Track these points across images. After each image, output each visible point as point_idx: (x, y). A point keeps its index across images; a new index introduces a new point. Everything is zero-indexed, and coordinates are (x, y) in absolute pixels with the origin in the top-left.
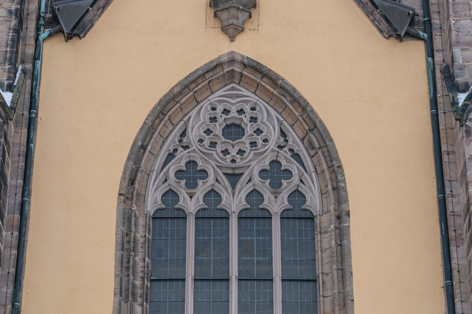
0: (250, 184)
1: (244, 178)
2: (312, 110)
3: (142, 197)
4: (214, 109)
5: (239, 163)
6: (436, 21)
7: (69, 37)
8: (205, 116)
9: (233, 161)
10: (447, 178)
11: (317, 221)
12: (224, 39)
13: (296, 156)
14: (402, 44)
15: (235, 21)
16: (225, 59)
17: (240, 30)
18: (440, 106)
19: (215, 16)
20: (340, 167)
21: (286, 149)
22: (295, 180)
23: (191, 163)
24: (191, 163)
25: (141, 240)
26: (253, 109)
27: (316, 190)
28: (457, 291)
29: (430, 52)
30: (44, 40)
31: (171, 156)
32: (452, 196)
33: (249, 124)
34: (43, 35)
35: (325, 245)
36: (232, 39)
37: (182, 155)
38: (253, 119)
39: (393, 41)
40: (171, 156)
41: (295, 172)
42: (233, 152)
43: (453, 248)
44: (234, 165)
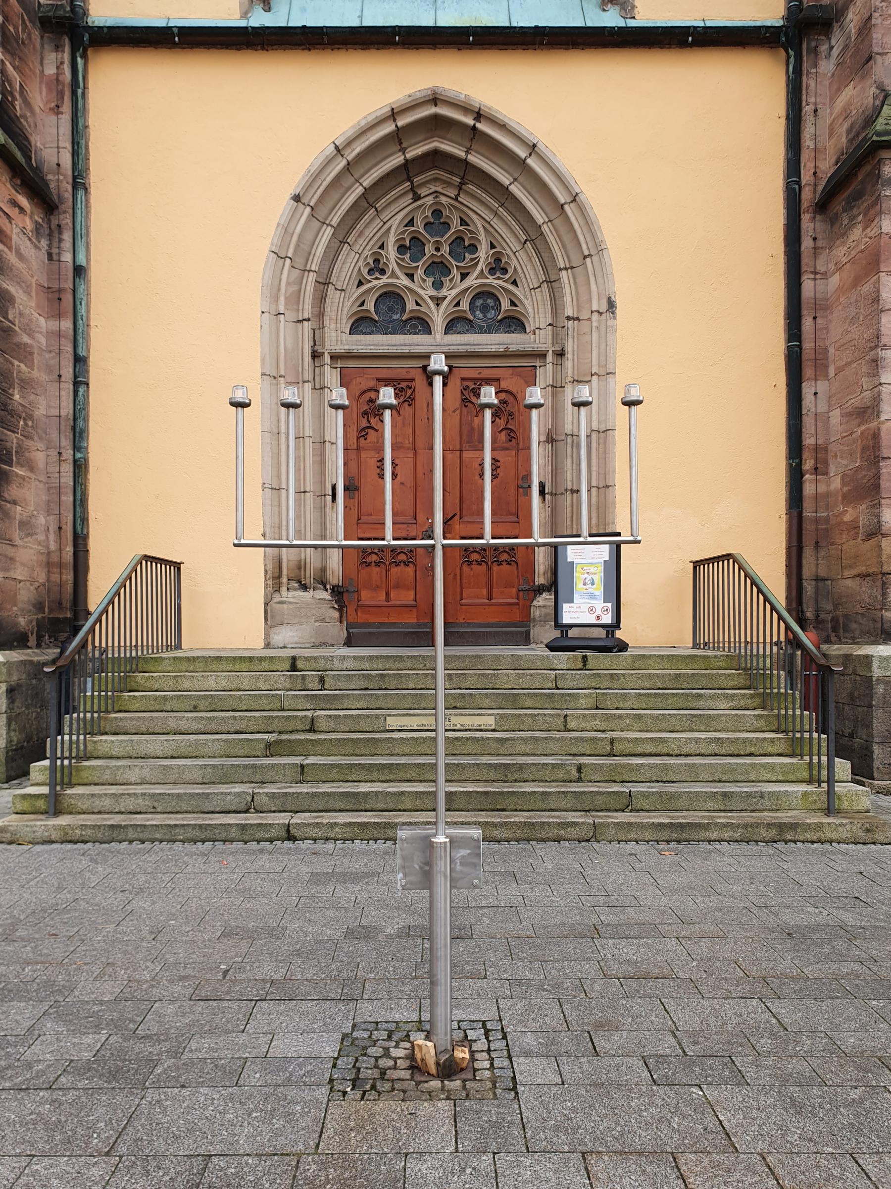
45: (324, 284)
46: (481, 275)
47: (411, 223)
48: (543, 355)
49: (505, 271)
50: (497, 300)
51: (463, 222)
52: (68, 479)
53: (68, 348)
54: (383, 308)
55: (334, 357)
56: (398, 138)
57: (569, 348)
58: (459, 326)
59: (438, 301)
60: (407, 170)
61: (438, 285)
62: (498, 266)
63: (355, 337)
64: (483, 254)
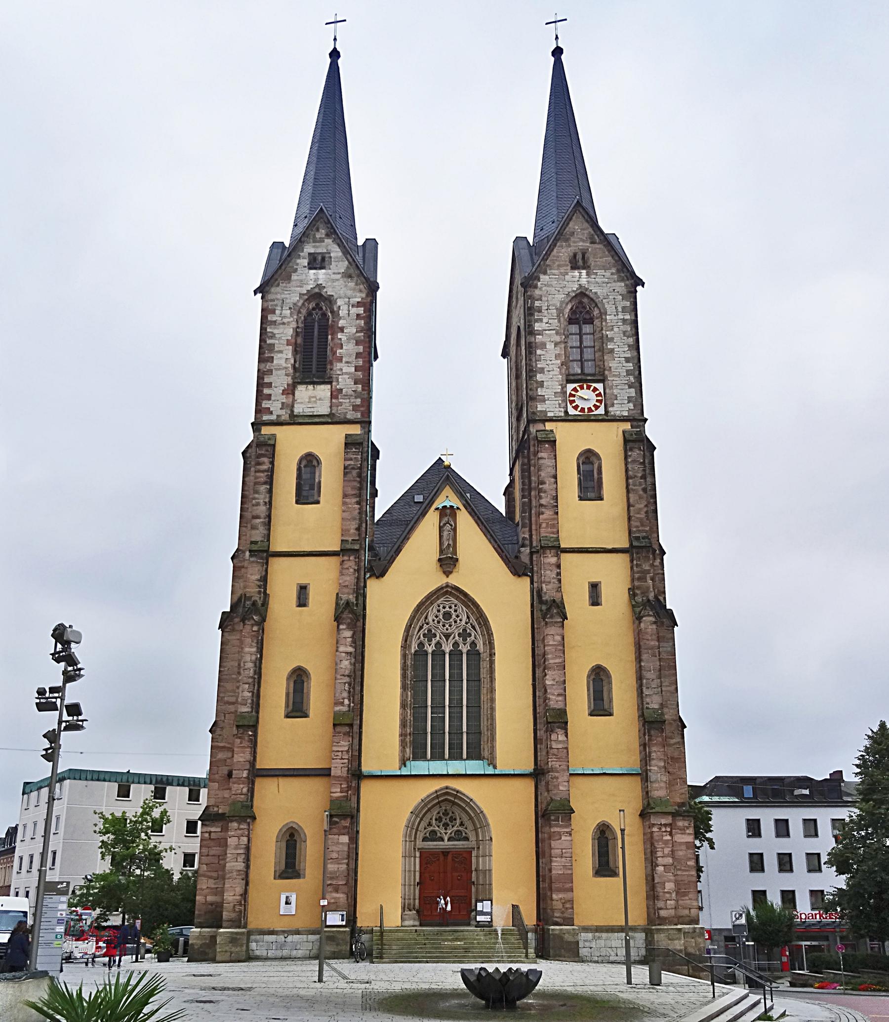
0: (454, 640)
2: (481, 609)
3: (410, 646)
4: (439, 606)
5: (449, 631)
6: (535, 569)
7: (377, 578)
8: (435, 611)
9: (447, 630)
10: (536, 639)
11: (482, 656)
13: (473, 627)
14: (520, 579)
15: (449, 569)
16: (444, 585)
17: (451, 572)
18: (535, 607)
19: (440, 566)
20: (492, 634)
21: (469, 624)
22: (473, 638)
23: (429, 631)
24: (429, 631)
25: (409, 665)
26: (455, 606)
28: (537, 687)
29: (532, 583)
30: (368, 578)
31: (421, 628)
32: (538, 647)
33: (454, 613)
35: (485, 666)
36: (448, 577)
37: (425, 626)
38: (456, 611)
39: (516, 577)
40: (421, 628)
41: (473, 635)
42: (447, 626)
43: (537, 669)
44: (447, 632)
45: (417, 830)
46: (457, 827)
47: (439, 813)
48: (474, 848)
49: (464, 825)
50: (462, 833)
51: (453, 813)
52: (353, 884)
53: (355, 851)
54: (431, 834)
55: (418, 849)
57: (481, 847)
58: (451, 839)
59: (446, 833)
60: (439, 803)
61: (446, 829)
62: (462, 824)
63: (425, 843)
64: (458, 821)
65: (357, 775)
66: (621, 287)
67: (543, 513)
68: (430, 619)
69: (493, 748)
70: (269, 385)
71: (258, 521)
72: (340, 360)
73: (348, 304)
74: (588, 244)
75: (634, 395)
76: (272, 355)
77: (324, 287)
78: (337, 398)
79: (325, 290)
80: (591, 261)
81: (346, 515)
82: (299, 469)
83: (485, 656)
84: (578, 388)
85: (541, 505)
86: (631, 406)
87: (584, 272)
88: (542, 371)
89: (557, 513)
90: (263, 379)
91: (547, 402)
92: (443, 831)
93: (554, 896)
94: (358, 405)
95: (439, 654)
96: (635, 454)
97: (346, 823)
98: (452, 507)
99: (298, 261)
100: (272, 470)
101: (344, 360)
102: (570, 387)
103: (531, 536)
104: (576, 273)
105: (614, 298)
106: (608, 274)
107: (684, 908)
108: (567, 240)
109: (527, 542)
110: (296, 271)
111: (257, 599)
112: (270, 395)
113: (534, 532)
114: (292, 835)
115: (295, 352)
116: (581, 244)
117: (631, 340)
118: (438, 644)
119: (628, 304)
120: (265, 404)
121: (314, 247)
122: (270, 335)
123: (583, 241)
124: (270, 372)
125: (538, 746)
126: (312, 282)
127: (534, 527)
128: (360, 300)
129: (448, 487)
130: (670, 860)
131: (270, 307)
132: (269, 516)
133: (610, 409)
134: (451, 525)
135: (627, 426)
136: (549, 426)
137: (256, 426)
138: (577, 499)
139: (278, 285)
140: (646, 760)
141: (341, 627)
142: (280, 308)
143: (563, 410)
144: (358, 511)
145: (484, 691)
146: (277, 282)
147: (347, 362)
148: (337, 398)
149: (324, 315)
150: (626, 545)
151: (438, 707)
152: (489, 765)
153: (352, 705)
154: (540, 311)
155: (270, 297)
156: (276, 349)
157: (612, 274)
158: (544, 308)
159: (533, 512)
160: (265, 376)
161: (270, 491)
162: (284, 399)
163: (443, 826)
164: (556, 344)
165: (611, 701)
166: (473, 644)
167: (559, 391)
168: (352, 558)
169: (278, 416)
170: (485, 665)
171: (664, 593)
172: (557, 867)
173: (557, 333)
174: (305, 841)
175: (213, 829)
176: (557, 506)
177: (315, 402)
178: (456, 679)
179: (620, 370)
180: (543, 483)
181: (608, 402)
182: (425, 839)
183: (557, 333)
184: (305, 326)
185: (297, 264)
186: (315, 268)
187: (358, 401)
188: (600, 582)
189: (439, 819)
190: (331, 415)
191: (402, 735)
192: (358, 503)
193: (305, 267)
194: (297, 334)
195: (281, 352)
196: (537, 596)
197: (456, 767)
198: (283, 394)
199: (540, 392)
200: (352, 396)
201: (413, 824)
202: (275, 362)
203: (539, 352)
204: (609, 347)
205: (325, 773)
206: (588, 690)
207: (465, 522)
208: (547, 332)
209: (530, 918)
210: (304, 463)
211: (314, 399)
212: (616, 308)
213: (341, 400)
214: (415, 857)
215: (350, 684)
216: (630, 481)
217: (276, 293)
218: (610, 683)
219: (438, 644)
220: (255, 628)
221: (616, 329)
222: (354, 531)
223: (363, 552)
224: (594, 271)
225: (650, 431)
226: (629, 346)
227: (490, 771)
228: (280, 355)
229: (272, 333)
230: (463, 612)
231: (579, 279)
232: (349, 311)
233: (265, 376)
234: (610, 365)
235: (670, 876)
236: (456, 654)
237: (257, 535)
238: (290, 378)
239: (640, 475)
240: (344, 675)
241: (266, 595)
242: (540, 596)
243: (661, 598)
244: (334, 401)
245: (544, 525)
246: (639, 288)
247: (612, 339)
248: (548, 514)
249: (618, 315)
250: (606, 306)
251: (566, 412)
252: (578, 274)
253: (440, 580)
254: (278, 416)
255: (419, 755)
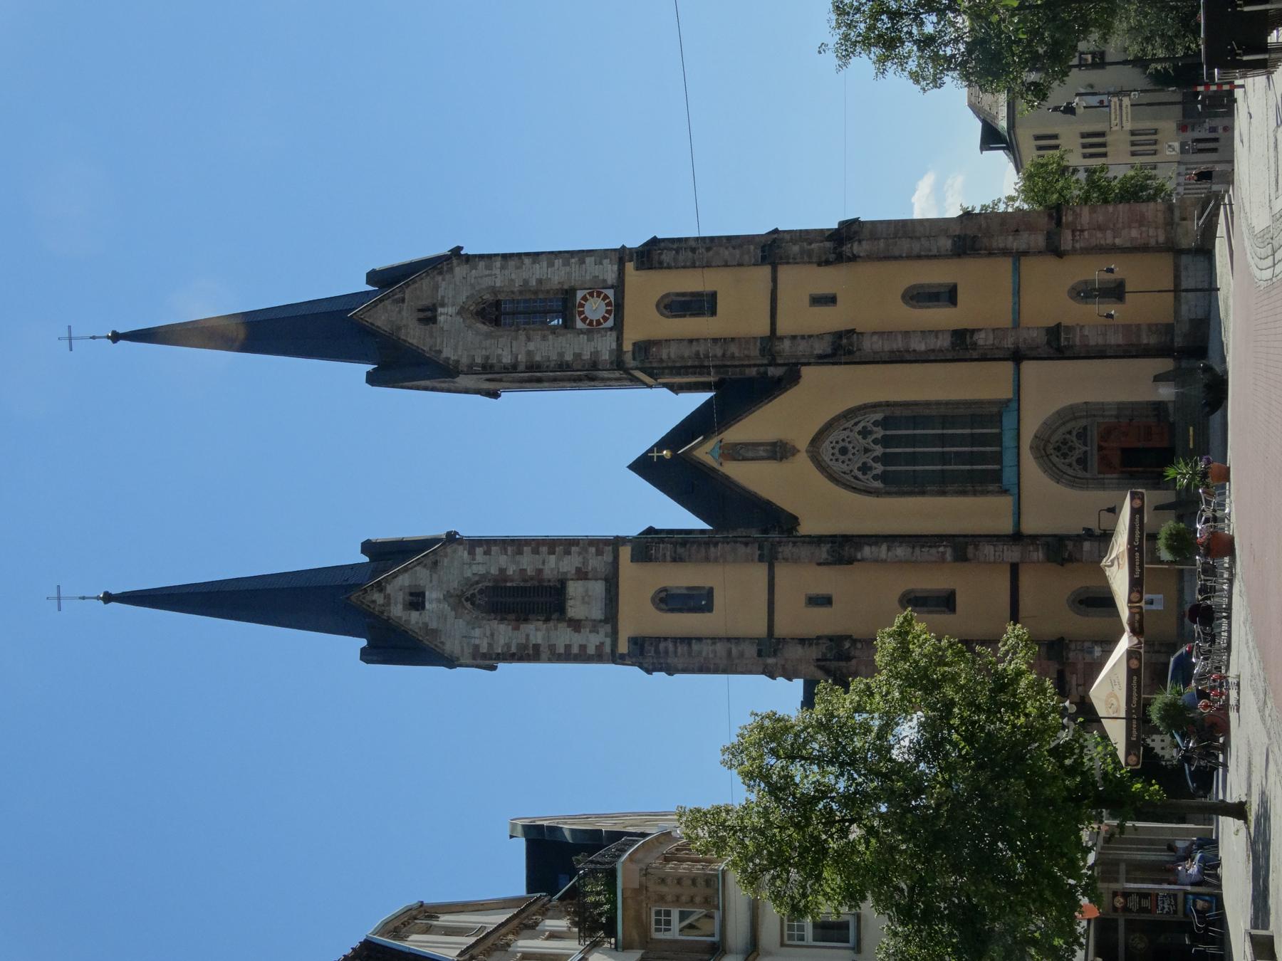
1: (869, 447)
3: (877, 488)
6: (793, 361)
12: (798, 455)
22: (869, 425)
23: (859, 469)
24: (859, 469)
26: (831, 443)
27: (872, 415)
29: (808, 364)
34: (798, 534)
36: (799, 451)
37: (856, 472)
38: (837, 442)
40: (856, 478)
47: (1057, 456)
56: (1042, 457)
59: (1079, 448)
60: (1048, 456)
61: (1075, 449)
62: (1070, 433)
65: (1017, 537)
66: (460, 271)
67: (733, 354)
68: (845, 467)
69: (991, 403)
70: (568, 647)
71: (734, 651)
72: (540, 571)
73: (470, 565)
74: (406, 304)
75: (593, 259)
76: (531, 646)
77: (448, 592)
78: (586, 573)
79: (452, 591)
80: (426, 302)
81: (721, 561)
82: (672, 610)
83: (888, 413)
84: (582, 316)
85: (724, 355)
86: (606, 262)
87: (440, 310)
88: (561, 355)
89: (733, 339)
90: (560, 655)
91: (599, 349)
92: (1077, 452)
93: (1145, 341)
94: (597, 550)
95: (886, 459)
96: (667, 257)
97: (1070, 545)
98: (720, 448)
99: (413, 621)
100: (676, 640)
101: (541, 567)
102: (579, 324)
103: (755, 365)
104: (441, 319)
105: (475, 278)
106: (443, 285)
107: (1156, 216)
108: (399, 328)
109: (762, 369)
110: (426, 625)
111: (824, 646)
112: (581, 646)
113: (752, 362)
114: (1081, 602)
115: (526, 620)
116: (404, 313)
117: (527, 261)
118: (875, 459)
119: (482, 264)
120: (591, 650)
121: (396, 604)
122: (505, 649)
123: (400, 312)
124: (552, 648)
125: (989, 357)
126: (441, 606)
127: (746, 363)
128: (466, 553)
129: (694, 453)
130: (1109, 234)
131: (471, 651)
132: (729, 639)
133: (610, 282)
134: (742, 448)
135: (630, 266)
136: (628, 346)
137: (617, 658)
138: (714, 318)
139: (443, 643)
140: (1005, 252)
141: (859, 556)
142: (473, 641)
143: (609, 333)
144: (725, 545)
145: (927, 412)
146: (439, 644)
147: (544, 563)
148: (586, 573)
149: (481, 592)
150: (766, 271)
151: (944, 458)
152: (1007, 406)
153: (945, 543)
154: (487, 358)
155: (457, 651)
156: (524, 641)
157: (443, 280)
158: (484, 352)
159: (729, 363)
160: (557, 652)
161: (699, 639)
162: (585, 631)
163: (1071, 451)
164: (529, 339)
165: (940, 285)
166: (876, 423)
167: (585, 337)
168: (780, 550)
169: (606, 636)
170: (898, 412)
171: (822, 230)
172: (1115, 339)
173: (516, 339)
174: (1088, 588)
175: (1074, 683)
176: (725, 339)
177: (590, 596)
178: (911, 441)
179: (563, 272)
180: (697, 354)
181: (601, 286)
182: (1085, 469)
183: (516, 339)
184: (493, 612)
185: (417, 623)
186: (423, 603)
187: (593, 550)
188: (810, 295)
189: (1065, 456)
190: (606, 580)
191: (975, 493)
192: (716, 544)
193: (421, 614)
194: (502, 620)
195: (528, 636)
196: (823, 359)
197: (1008, 440)
198: (579, 632)
199: (586, 356)
200: (584, 558)
201: (1071, 481)
202: (539, 641)
203: (538, 358)
204: (534, 284)
205: (1015, 569)
206: (929, 307)
207: (737, 433)
208: (514, 350)
209: (1165, 365)
210: (663, 606)
211: (586, 599)
212: (486, 276)
213: (590, 568)
214: (1104, 479)
215: (923, 546)
216: (697, 264)
217: (452, 646)
218: (922, 286)
219: (875, 459)
220: (859, 646)
221: (513, 276)
222: (749, 548)
223: (771, 540)
224: (439, 298)
225: (635, 242)
226: (534, 262)
227: (1014, 405)
228: (532, 637)
229: (503, 647)
230: (837, 435)
231: (446, 315)
232: (479, 564)
233: (557, 652)
234: (556, 282)
235: (1124, 233)
236: (886, 441)
237: (751, 651)
238: (560, 625)
239: (690, 254)
240: (913, 552)
241: (819, 638)
242: (826, 356)
243: (830, 232)
244: (590, 576)
245: (746, 352)
246: (462, 252)
247: (526, 282)
248: (733, 349)
249: (495, 274)
250: (484, 286)
251: (611, 329)
252: (443, 317)
253: (802, 461)
254: (606, 637)
255: (996, 477)
